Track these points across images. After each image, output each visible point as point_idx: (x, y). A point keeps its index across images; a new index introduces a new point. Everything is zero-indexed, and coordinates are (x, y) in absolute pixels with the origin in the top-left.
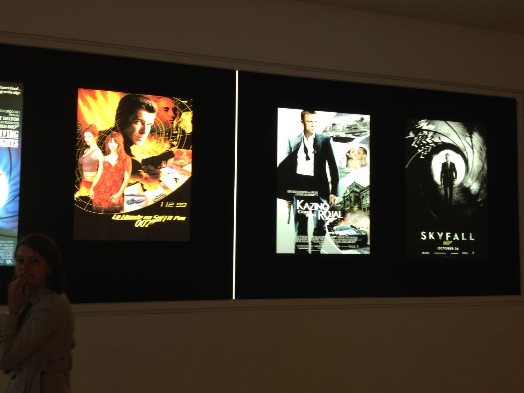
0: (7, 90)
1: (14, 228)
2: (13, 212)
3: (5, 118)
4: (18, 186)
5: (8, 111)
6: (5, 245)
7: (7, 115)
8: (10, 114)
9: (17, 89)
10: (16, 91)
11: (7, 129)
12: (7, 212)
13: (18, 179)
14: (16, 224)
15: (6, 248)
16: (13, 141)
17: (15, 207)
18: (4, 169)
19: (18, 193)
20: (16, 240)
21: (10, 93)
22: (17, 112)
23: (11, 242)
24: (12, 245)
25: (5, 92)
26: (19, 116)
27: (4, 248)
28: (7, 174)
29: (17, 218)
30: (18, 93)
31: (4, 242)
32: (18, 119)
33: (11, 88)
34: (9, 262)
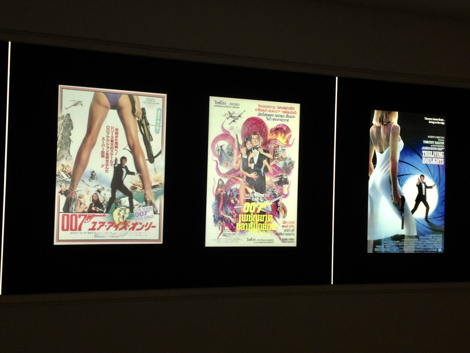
0: (437, 121)
1: (442, 225)
2: (441, 213)
3: (436, 143)
4: (444, 194)
5: (438, 137)
6: (438, 238)
7: (437, 140)
8: (439, 140)
9: (442, 120)
10: (441, 121)
11: (437, 151)
12: (439, 213)
13: (444, 188)
14: (443, 222)
15: (438, 240)
16: (441, 159)
17: (442, 209)
18: (436, 181)
19: (444, 198)
20: (443, 234)
21: (439, 123)
22: (443, 138)
23: (441, 235)
24: (441, 238)
25: (436, 123)
26: (443, 140)
27: (437, 240)
28: (437, 186)
29: (443, 217)
30: (443, 123)
31: (436, 235)
32: (443, 143)
33: (440, 120)
34: (440, 250)
